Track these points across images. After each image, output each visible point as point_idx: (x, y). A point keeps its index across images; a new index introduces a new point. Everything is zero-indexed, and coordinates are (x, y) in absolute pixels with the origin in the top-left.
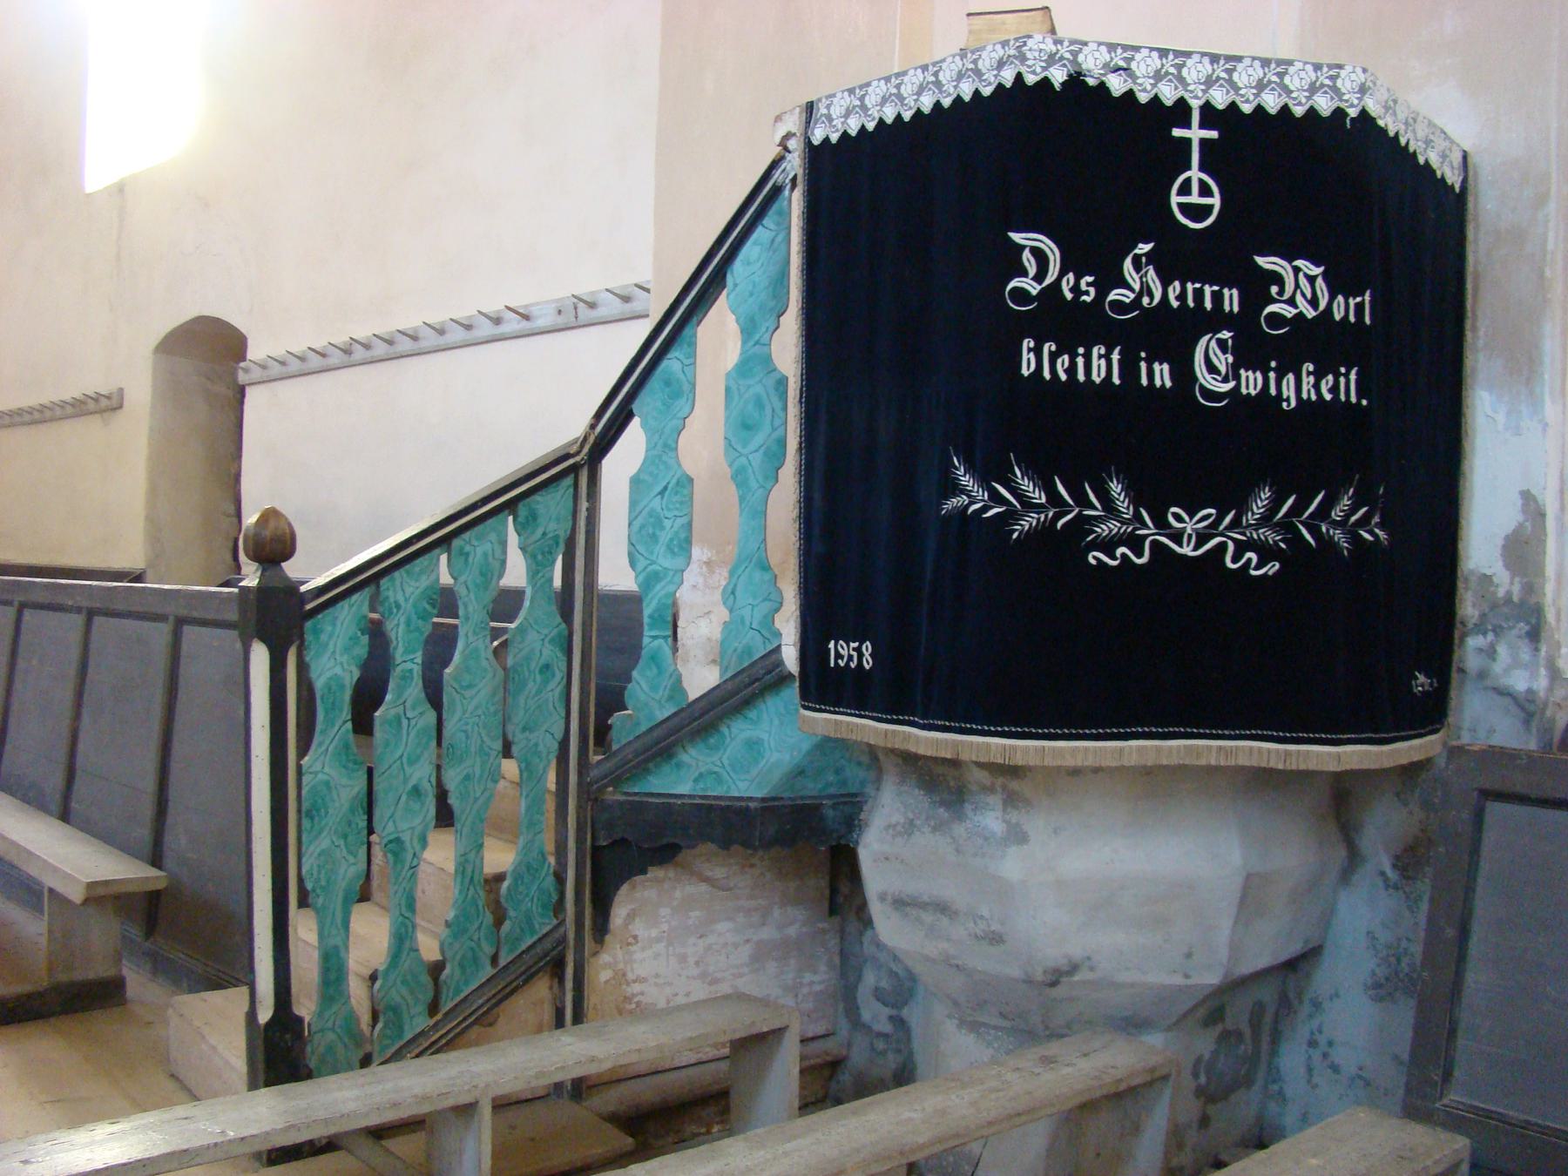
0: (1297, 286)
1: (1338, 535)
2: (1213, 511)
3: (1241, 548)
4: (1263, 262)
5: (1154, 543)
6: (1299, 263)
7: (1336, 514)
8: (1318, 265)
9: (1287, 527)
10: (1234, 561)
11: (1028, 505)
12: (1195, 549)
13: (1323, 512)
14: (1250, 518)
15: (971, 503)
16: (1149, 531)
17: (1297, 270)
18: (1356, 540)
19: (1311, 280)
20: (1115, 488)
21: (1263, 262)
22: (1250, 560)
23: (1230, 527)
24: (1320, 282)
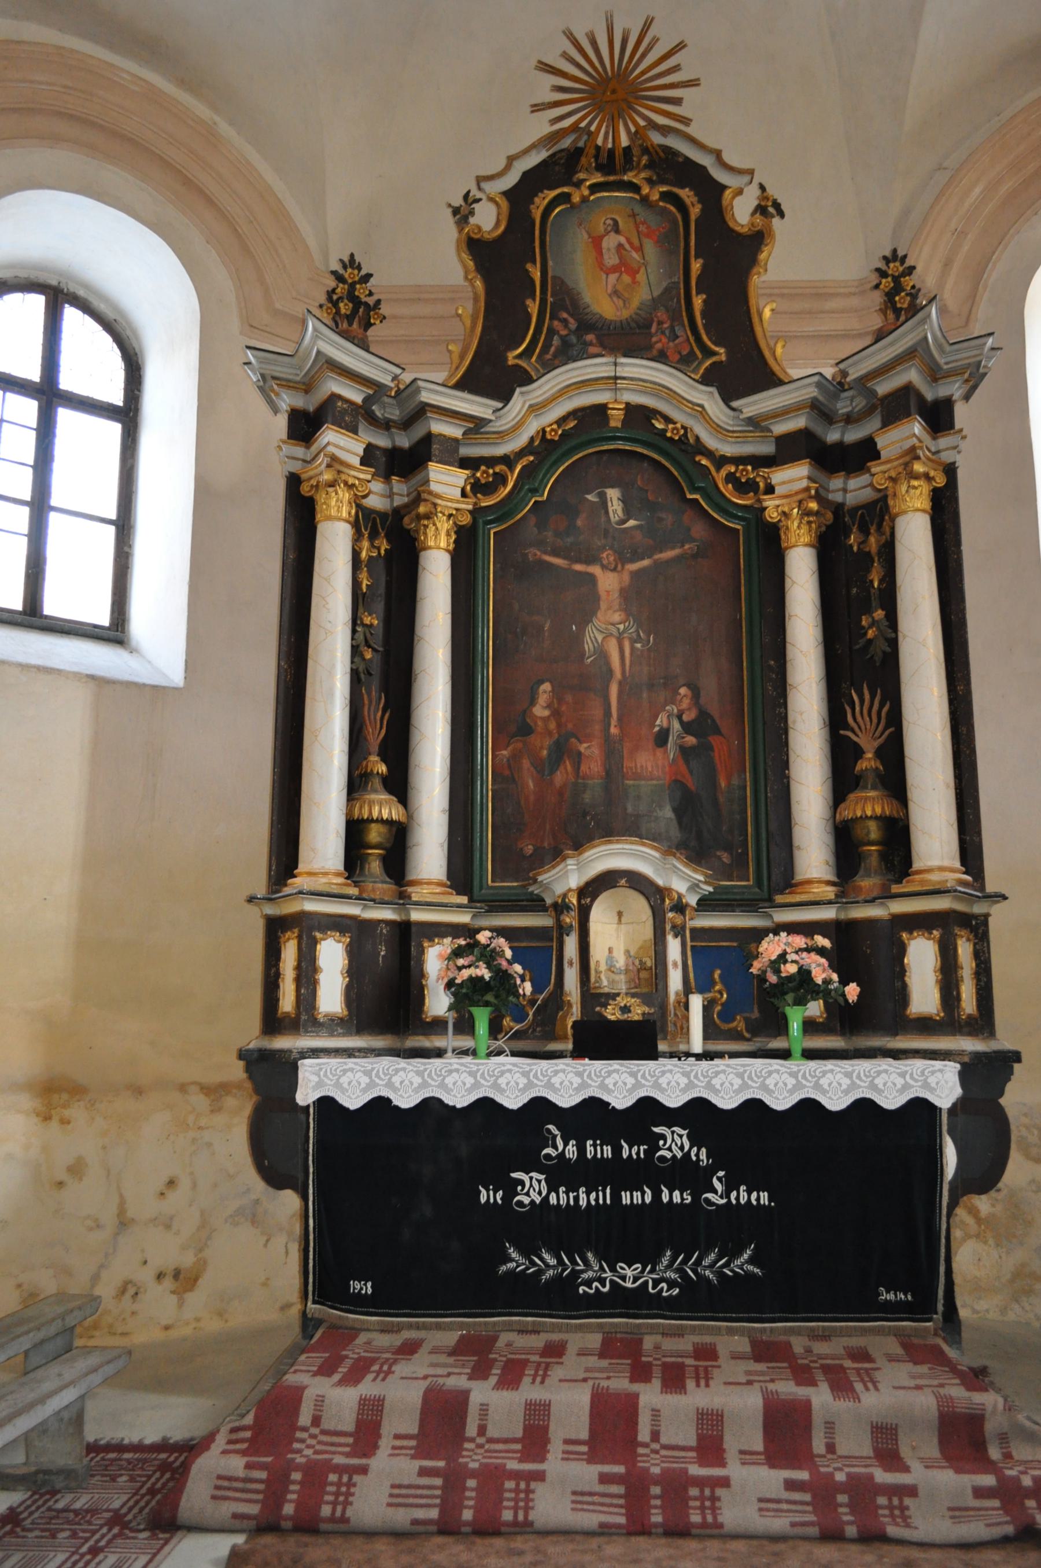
0: (673, 1140)
1: (707, 1272)
2: (639, 1265)
3: (656, 1283)
4: (656, 1130)
5: (612, 1282)
6: (674, 1129)
7: (706, 1262)
8: (685, 1129)
9: (681, 1271)
10: (653, 1289)
11: (547, 1265)
12: (634, 1282)
13: (698, 1262)
14: (660, 1267)
15: (518, 1266)
16: (608, 1274)
17: (673, 1132)
18: (720, 1274)
19: (681, 1136)
20: (590, 1255)
21: (656, 1130)
22: (662, 1288)
23: (651, 1272)
24: (685, 1138)
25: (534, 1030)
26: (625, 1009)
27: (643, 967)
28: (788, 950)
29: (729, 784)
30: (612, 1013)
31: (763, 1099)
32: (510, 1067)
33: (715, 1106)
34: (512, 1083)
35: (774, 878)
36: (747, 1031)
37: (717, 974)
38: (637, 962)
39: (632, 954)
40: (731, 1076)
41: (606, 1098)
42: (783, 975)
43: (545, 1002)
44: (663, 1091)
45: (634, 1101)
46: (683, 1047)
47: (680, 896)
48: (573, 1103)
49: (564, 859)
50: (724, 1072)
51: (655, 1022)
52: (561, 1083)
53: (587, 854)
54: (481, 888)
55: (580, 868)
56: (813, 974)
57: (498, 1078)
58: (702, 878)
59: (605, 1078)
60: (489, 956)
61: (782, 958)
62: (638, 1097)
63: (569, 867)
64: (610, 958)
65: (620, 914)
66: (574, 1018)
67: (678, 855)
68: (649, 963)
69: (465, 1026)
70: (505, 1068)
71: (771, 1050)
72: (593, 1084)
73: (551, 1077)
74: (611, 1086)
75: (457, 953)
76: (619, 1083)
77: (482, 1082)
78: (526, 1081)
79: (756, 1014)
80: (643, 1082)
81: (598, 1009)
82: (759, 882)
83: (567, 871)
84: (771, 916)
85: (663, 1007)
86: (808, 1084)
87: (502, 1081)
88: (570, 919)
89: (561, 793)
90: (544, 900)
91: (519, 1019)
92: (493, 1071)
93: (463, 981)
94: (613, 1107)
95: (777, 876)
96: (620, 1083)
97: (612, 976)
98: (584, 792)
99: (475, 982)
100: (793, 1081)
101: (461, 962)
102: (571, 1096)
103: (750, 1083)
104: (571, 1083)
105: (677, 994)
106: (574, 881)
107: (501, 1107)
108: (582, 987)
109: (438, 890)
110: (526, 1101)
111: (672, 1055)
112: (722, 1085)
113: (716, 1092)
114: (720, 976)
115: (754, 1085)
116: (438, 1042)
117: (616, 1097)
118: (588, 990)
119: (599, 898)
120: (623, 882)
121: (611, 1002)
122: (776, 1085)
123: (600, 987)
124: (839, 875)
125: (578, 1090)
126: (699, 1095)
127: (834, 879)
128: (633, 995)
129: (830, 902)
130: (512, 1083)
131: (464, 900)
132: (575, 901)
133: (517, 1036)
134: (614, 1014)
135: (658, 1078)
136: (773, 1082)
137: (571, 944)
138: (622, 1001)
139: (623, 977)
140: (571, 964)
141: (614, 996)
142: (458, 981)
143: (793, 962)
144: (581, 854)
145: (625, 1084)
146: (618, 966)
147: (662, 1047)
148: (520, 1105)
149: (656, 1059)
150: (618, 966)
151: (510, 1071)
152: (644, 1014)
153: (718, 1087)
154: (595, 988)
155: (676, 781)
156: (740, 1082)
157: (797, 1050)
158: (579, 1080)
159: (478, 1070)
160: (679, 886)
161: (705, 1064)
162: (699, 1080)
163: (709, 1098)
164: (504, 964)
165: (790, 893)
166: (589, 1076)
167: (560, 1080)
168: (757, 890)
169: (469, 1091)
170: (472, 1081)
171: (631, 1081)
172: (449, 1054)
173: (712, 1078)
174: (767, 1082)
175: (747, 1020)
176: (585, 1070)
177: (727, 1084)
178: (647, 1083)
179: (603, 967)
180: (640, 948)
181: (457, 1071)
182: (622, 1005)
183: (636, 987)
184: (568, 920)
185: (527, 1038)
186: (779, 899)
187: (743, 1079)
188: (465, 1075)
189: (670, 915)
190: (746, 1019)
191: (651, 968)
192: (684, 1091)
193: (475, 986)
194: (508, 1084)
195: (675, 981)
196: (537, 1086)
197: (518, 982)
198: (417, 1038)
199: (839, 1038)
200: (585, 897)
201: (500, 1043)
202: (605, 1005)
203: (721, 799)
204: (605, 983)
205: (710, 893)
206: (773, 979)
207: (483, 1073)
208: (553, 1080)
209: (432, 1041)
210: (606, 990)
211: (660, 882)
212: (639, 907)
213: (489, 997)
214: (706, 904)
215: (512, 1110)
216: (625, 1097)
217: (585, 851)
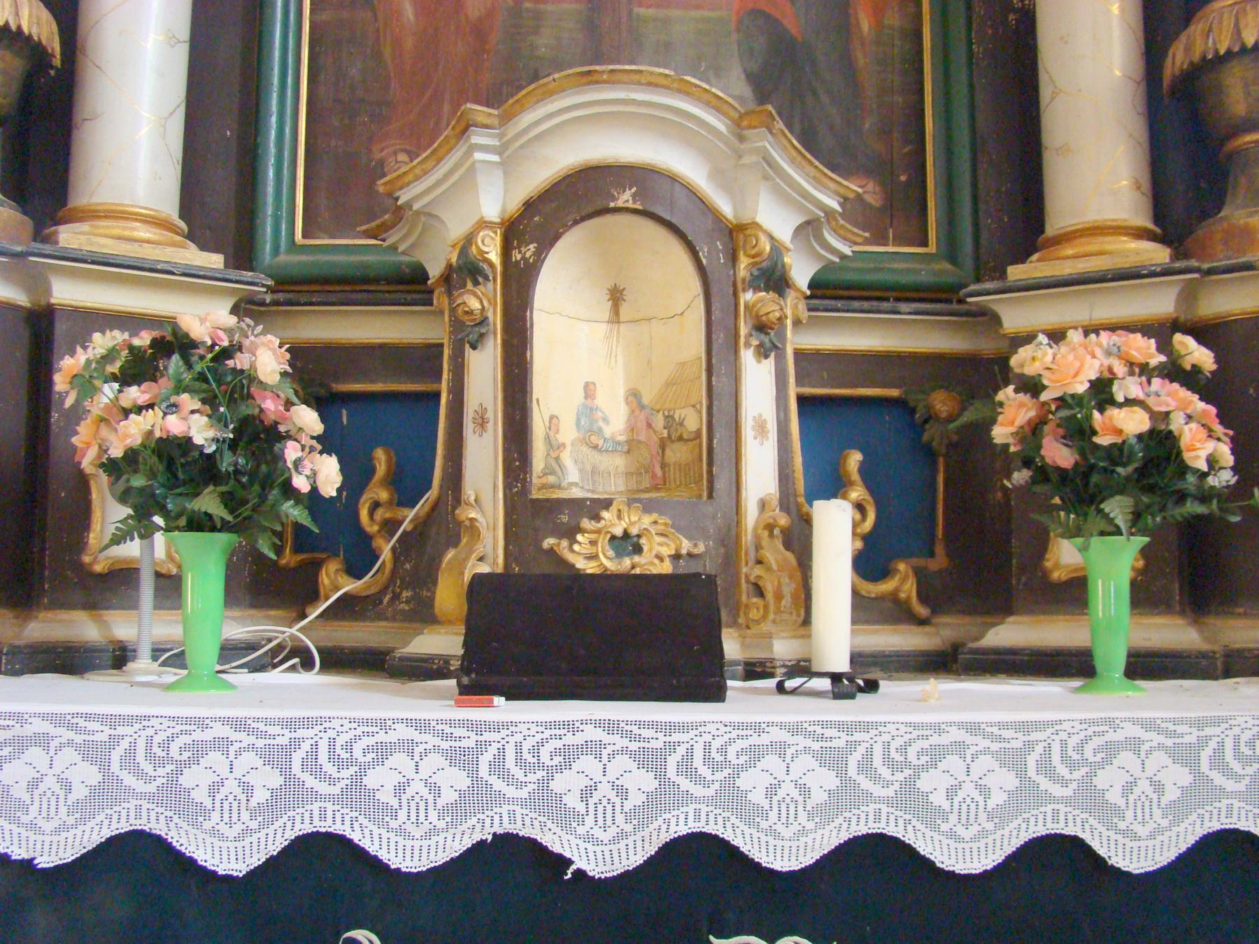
25: (396, 597)
26: (627, 543)
27: (674, 434)
28: (1120, 369)
29: (878, 25)
30: (588, 555)
31: (1086, 836)
32: (221, 731)
33: (926, 864)
34: (231, 786)
35: (984, 240)
36: (923, 598)
37: (854, 459)
38: (659, 422)
39: (645, 401)
40: (985, 762)
41: (555, 841)
42: (1103, 440)
43: (423, 525)
44: (751, 814)
45: (652, 850)
46: (783, 649)
47: (778, 249)
48: (441, 858)
49: (465, 130)
50: (959, 748)
51: (711, 579)
52: (400, 789)
53: (527, 118)
54: (276, 250)
55: (509, 161)
56: (1184, 442)
57: (181, 767)
58: (834, 204)
59: (551, 772)
60: (221, 381)
61: (1102, 391)
62: (665, 837)
63: (478, 156)
64: (588, 412)
65: (616, 296)
66: (484, 569)
67: (780, 125)
68: (693, 421)
69: (170, 587)
70: (207, 735)
71: (997, 651)
72: (511, 792)
73: (363, 770)
74: (573, 801)
75: (138, 369)
76: (599, 782)
77: (129, 780)
78: (276, 780)
79: (940, 561)
80: (685, 784)
81: (549, 542)
82: (951, 252)
83: (472, 170)
84: (996, 320)
85: (729, 540)
86: (1230, 785)
87: (196, 779)
88: (482, 301)
89: (479, 32)
90: (425, 277)
91: (355, 571)
92: (165, 745)
93: (132, 457)
94: (580, 873)
95: (1017, 214)
96: (604, 790)
97: (596, 457)
98: (536, 31)
99: (172, 454)
100: (1184, 777)
101: (135, 394)
102: (433, 831)
103: (1044, 783)
104: (436, 790)
105: (763, 505)
106: (494, 200)
107: (187, 865)
108: (507, 487)
109: (144, 232)
110: (275, 848)
111: (754, 671)
112: (951, 793)
113: (933, 816)
114: (863, 470)
115: (1057, 791)
116: (122, 627)
117: (589, 838)
118: (525, 491)
119: (560, 244)
120: (625, 198)
121: (586, 523)
122: (1128, 788)
123: (559, 487)
124: (1159, 214)
125: (457, 812)
126: (874, 828)
127: (1150, 225)
128: (648, 507)
129: (1165, 273)
130: (231, 786)
131: (215, 261)
132: (494, 256)
133: (347, 608)
134: (593, 557)
135: (738, 770)
136: (1120, 779)
137: (483, 370)
138: (613, 522)
139: (618, 462)
140: (482, 423)
141: (594, 508)
142: (117, 452)
143: (1129, 402)
144: (506, 119)
145: (622, 792)
146: (608, 431)
147: (732, 647)
148: (256, 860)
149: (715, 693)
150: (608, 431)
151: (222, 744)
152: (676, 557)
153: (939, 799)
154: (544, 487)
155: (756, 13)
156: (1010, 780)
157: (1112, 657)
158: (462, 780)
159: (114, 741)
160: (776, 221)
161: (861, 708)
162: (876, 778)
163: (909, 839)
164: (271, 406)
165: (1039, 260)
166: (498, 766)
167: (392, 780)
168: (947, 266)
169: (84, 810)
170: (92, 775)
171: (641, 782)
172: (142, 666)
173: (918, 771)
174: (1101, 780)
175: (921, 575)
176: (482, 746)
177: (968, 789)
178: (698, 791)
179: (568, 433)
180: (669, 384)
181: (42, 741)
182: (618, 531)
183: (656, 488)
184: (474, 304)
185: (381, 617)
186: (1016, 272)
187: (1021, 773)
188: (69, 755)
189: (748, 297)
190: (919, 573)
191: (698, 434)
192: (823, 814)
193: (170, 466)
194: (214, 789)
195: (760, 472)
196: (315, 796)
197: (292, 452)
198: (64, 615)
199: (1179, 621)
200: (523, 243)
201: (294, 630)
202: (571, 533)
203: (861, 60)
204: (573, 475)
205: (843, 257)
206: (1059, 454)
207: (131, 752)
208: (371, 780)
209: (103, 624)
210: (576, 493)
211: (726, 208)
212: (669, 278)
213: (209, 502)
214: (830, 291)
215: (228, 879)
216: (622, 835)
217: (521, 107)
